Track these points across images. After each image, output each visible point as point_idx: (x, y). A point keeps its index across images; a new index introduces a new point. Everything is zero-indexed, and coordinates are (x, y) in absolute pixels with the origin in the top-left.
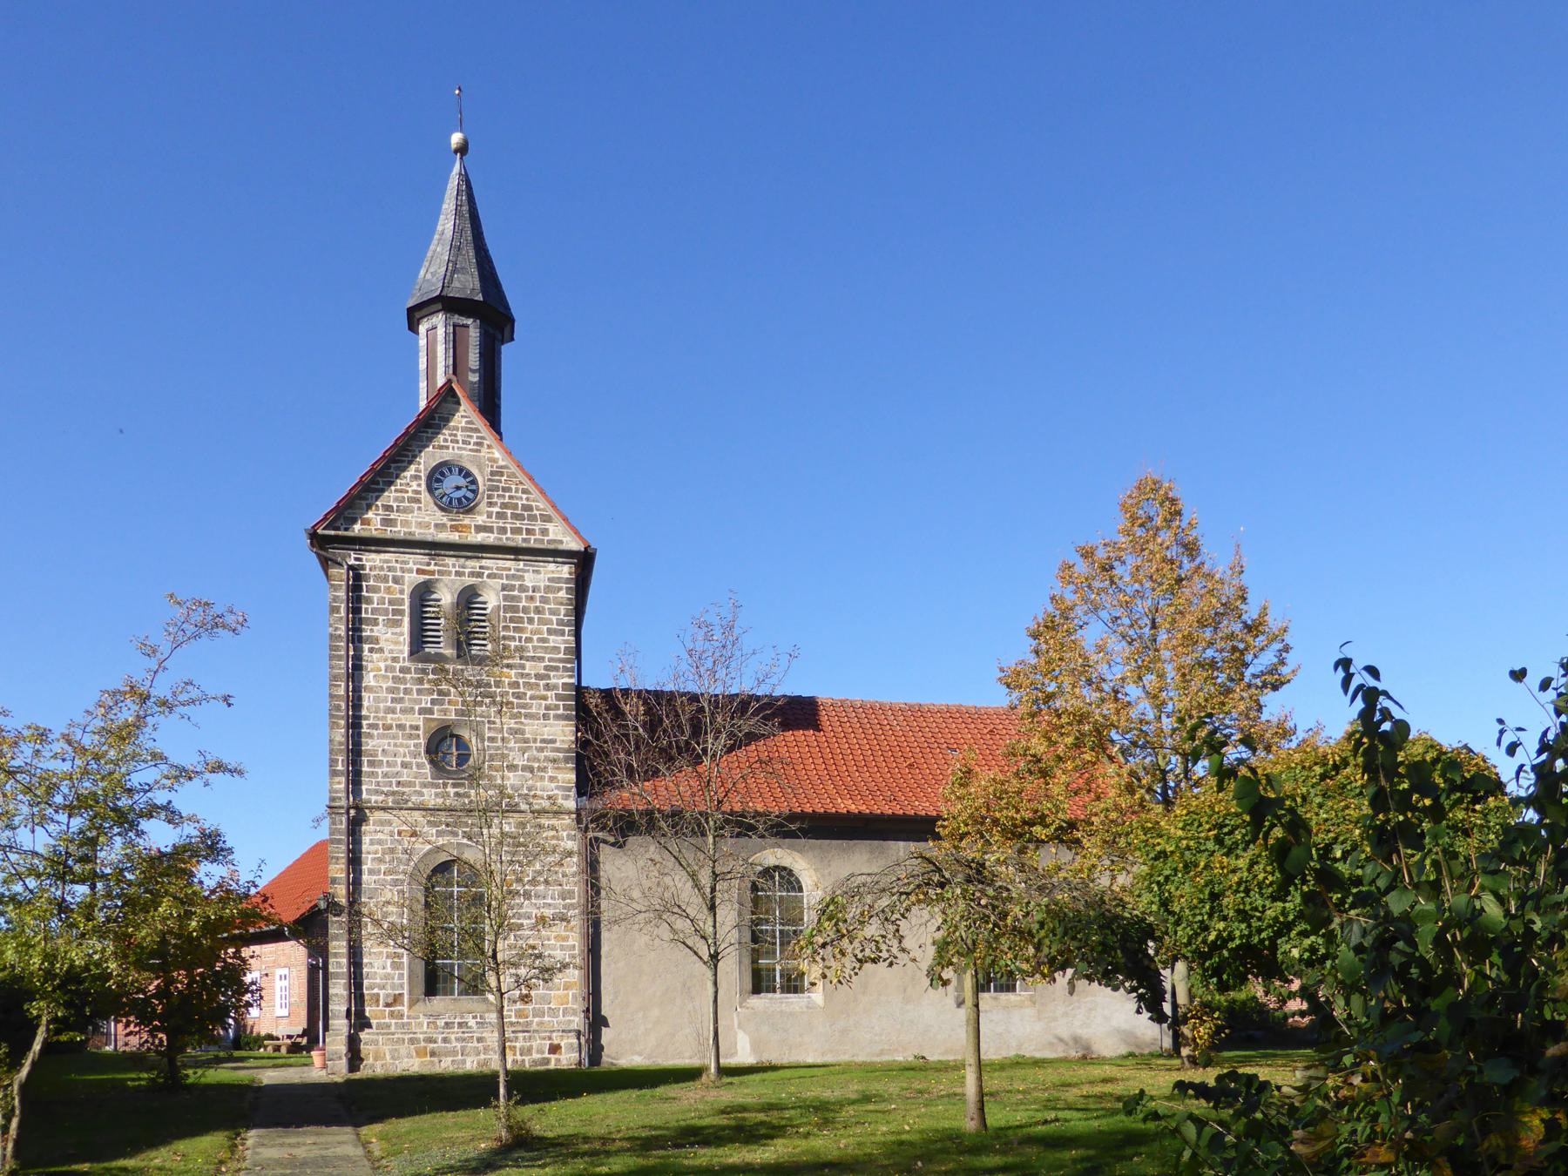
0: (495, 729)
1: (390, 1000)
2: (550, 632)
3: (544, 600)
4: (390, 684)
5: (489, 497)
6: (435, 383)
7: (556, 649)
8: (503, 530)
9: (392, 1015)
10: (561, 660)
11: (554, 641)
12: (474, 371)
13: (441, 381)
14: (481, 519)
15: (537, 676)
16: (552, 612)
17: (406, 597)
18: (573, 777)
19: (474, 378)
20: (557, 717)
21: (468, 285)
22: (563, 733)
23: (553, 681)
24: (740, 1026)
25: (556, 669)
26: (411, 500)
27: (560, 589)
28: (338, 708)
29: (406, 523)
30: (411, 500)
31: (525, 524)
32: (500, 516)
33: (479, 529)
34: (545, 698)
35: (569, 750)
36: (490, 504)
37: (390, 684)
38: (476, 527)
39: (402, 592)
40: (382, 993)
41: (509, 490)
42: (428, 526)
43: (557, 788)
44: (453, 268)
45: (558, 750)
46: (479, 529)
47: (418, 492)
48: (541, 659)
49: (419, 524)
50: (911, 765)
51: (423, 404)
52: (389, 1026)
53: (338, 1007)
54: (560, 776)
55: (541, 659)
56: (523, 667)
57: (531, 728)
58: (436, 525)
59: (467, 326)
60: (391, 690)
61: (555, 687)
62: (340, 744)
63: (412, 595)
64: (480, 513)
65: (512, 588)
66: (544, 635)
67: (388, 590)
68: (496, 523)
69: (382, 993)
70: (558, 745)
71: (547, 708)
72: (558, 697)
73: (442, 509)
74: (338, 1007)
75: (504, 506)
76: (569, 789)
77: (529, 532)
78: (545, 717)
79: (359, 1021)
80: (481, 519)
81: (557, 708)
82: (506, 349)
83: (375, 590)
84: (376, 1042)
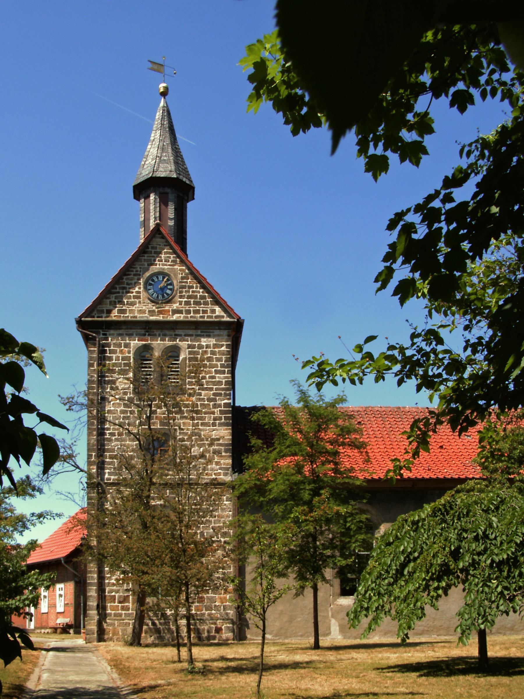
0: (183, 433)
1: (122, 600)
2: (217, 372)
3: (213, 353)
4: (122, 408)
5: (181, 292)
6: (149, 227)
7: (220, 383)
8: (188, 312)
9: (123, 608)
10: (223, 389)
11: (219, 377)
12: (171, 219)
13: (152, 224)
14: (175, 306)
15: (209, 400)
16: (218, 360)
17: (131, 355)
18: (230, 461)
19: (171, 223)
20: (221, 425)
21: (167, 170)
22: (224, 433)
23: (218, 402)
24: (333, 616)
25: (220, 395)
26: (135, 297)
27: (222, 346)
28: (93, 424)
29: (131, 311)
30: (135, 297)
31: (202, 308)
32: (187, 303)
33: (175, 312)
34: (213, 413)
35: (227, 445)
36: (181, 297)
37: (122, 408)
38: (175, 312)
39: (129, 352)
40: (117, 595)
41: (192, 287)
42: (144, 312)
43: (220, 469)
44: (160, 160)
45: (221, 445)
46: (175, 312)
47: (139, 292)
48: (211, 389)
49: (140, 311)
50: (441, 447)
51: (142, 241)
52: (121, 615)
53: (93, 603)
54: (222, 461)
55: (211, 389)
56: (200, 394)
57: (205, 431)
58: (149, 311)
59: (167, 193)
60: (122, 412)
61: (220, 406)
62: (93, 445)
63: (135, 354)
64: (175, 303)
65: (193, 347)
66: (216, 374)
67: (121, 352)
68: (183, 307)
69: (117, 595)
70: (221, 442)
71: (215, 419)
72: (221, 412)
73: (152, 302)
74: (93, 603)
75: (189, 297)
76: (227, 469)
77: (204, 312)
78: (214, 425)
79: (101, 608)
80: (175, 306)
81: (220, 418)
82: (190, 205)
83: (114, 352)
84: (113, 625)
